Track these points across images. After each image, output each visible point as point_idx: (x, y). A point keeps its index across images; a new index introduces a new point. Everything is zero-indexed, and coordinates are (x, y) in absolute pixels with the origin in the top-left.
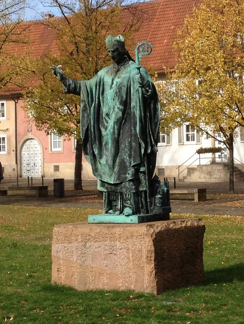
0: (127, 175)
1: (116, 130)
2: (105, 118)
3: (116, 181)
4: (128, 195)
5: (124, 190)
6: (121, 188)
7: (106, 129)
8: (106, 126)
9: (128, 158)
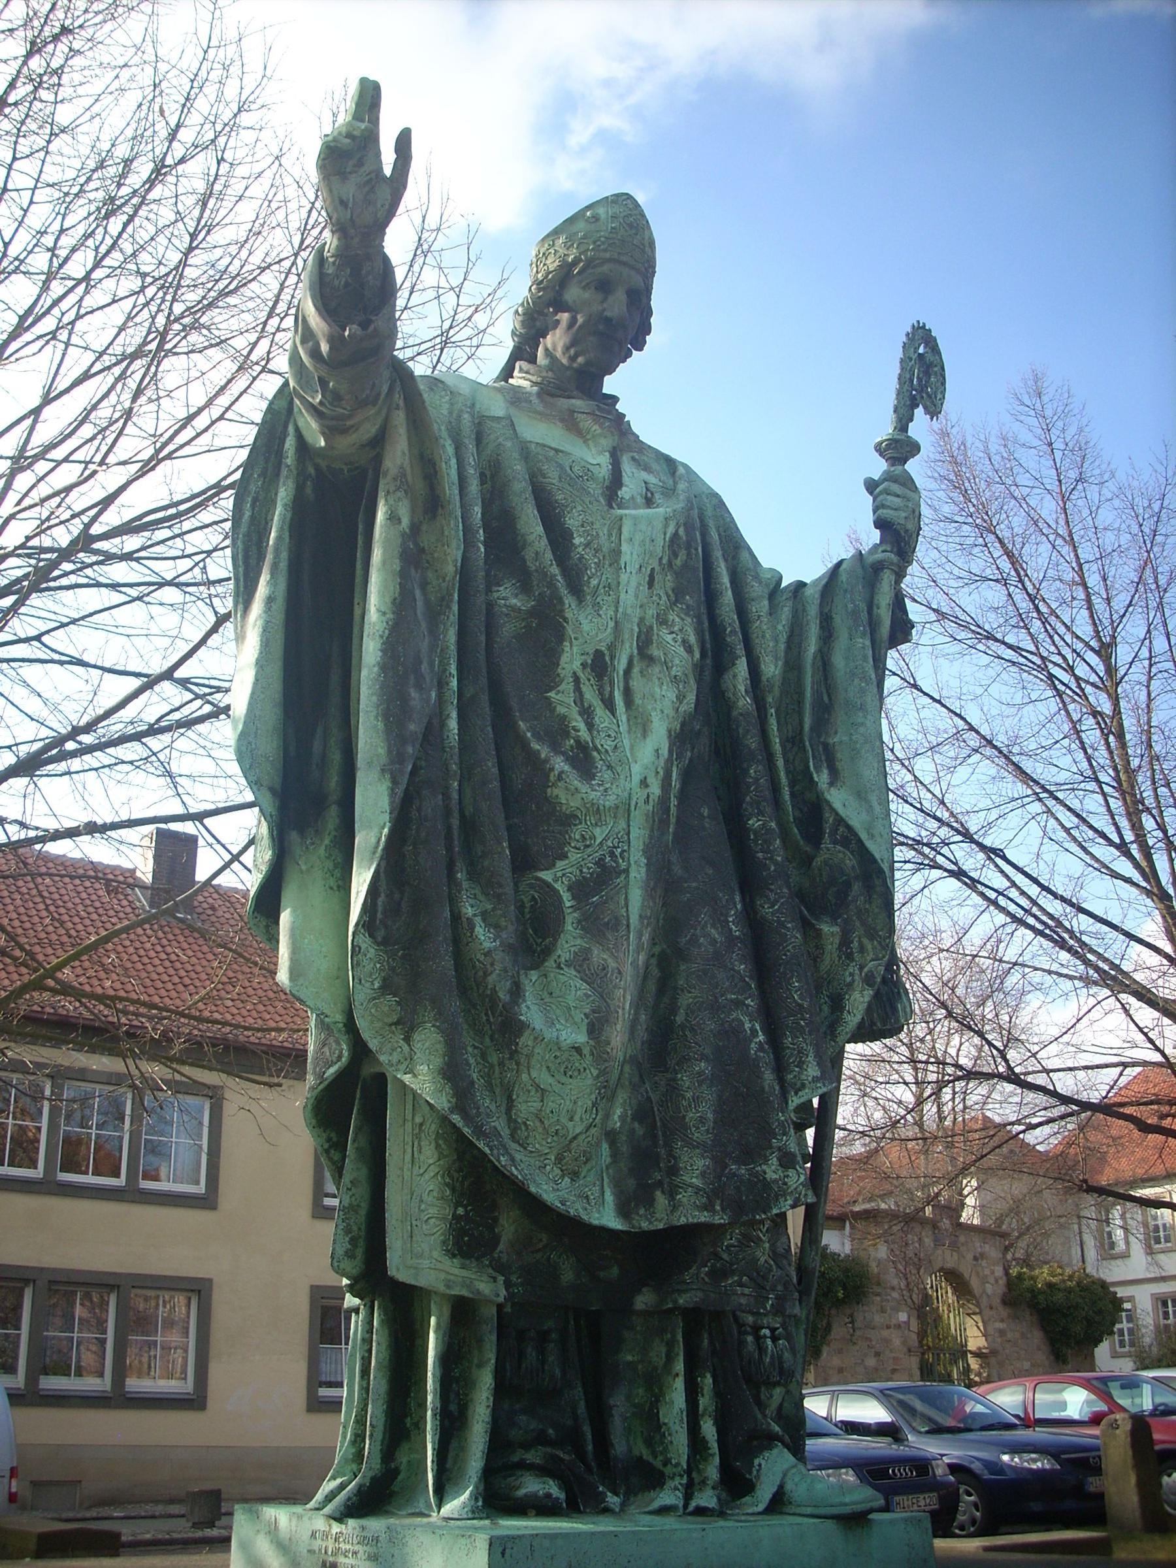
0: (771, 1170)
1: (674, 802)
2: (577, 680)
3: (708, 1207)
4: (775, 1339)
5: (742, 1294)
6: (718, 1275)
8: (581, 746)
9: (761, 1038)
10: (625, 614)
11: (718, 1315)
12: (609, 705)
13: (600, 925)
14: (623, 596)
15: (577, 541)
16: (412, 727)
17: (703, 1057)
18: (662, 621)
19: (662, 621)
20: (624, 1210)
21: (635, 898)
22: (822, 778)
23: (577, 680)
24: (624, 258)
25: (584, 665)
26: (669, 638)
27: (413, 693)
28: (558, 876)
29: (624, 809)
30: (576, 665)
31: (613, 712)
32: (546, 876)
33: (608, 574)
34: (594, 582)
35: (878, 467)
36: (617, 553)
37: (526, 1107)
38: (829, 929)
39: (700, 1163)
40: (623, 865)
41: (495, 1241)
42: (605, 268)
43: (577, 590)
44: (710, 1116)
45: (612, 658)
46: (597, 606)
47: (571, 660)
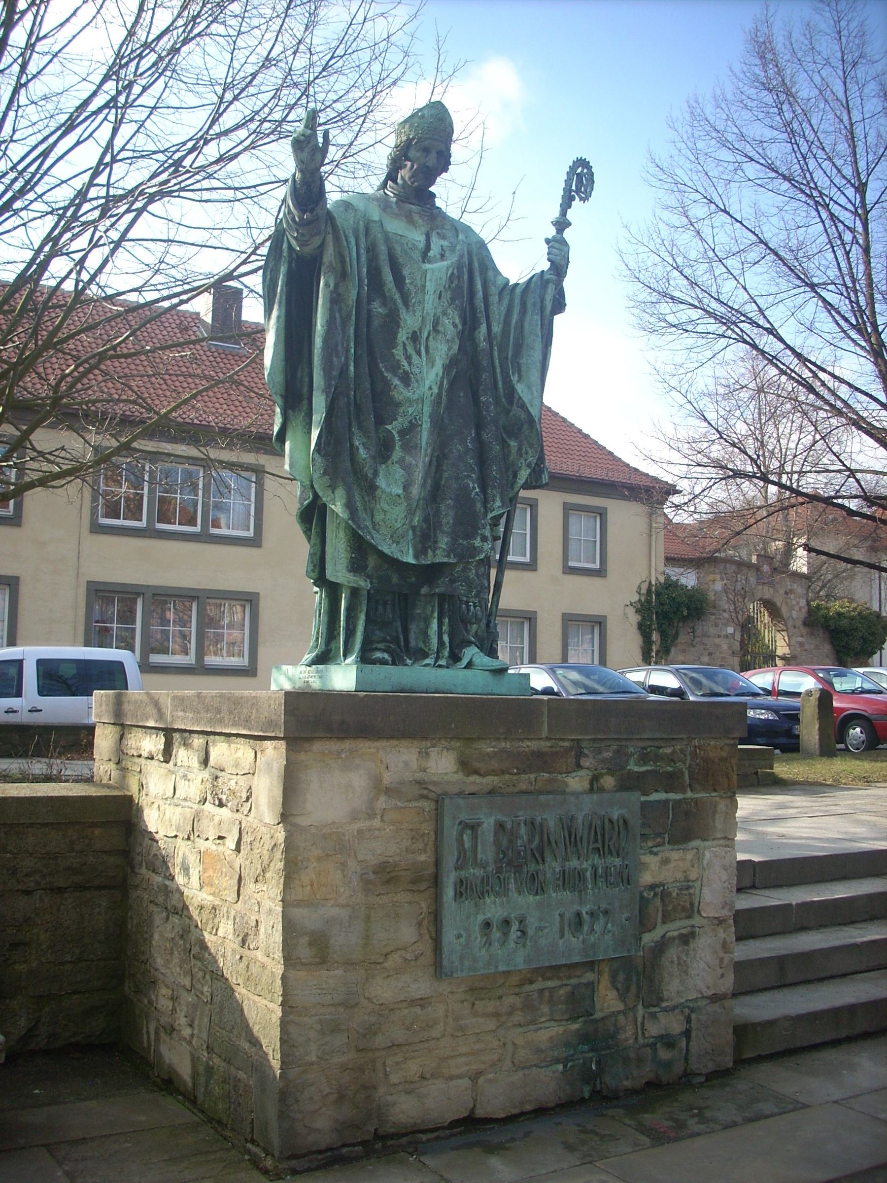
0: (477, 542)
1: (444, 394)
2: (404, 344)
3: (448, 556)
4: (475, 607)
5: (462, 589)
6: (452, 581)
7: (406, 379)
8: (406, 373)
9: (477, 490)
10: (427, 313)
11: (451, 597)
12: (419, 353)
13: (410, 447)
14: (426, 305)
15: (407, 281)
16: (334, 373)
17: (451, 498)
18: (445, 313)
19: (445, 313)
20: (416, 556)
21: (424, 435)
22: (515, 379)
23: (404, 344)
24: (436, 137)
25: (407, 338)
26: (447, 321)
27: (335, 359)
28: (393, 428)
29: (421, 400)
30: (404, 338)
31: (420, 356)
32: (389, 427)
33: (420, 296)
34: (413, 301)
35: (552, 232)
36: (424, 286)
37: (378, 517)
38: (513, 443)
39: (446, 540)
40: (420, 423)
41: (366, 566)
42: (427, 143)
43: (406, 303)
44: (451, 521)
45: (421, 333)
46: (414, 311)
47: (402, 336)
